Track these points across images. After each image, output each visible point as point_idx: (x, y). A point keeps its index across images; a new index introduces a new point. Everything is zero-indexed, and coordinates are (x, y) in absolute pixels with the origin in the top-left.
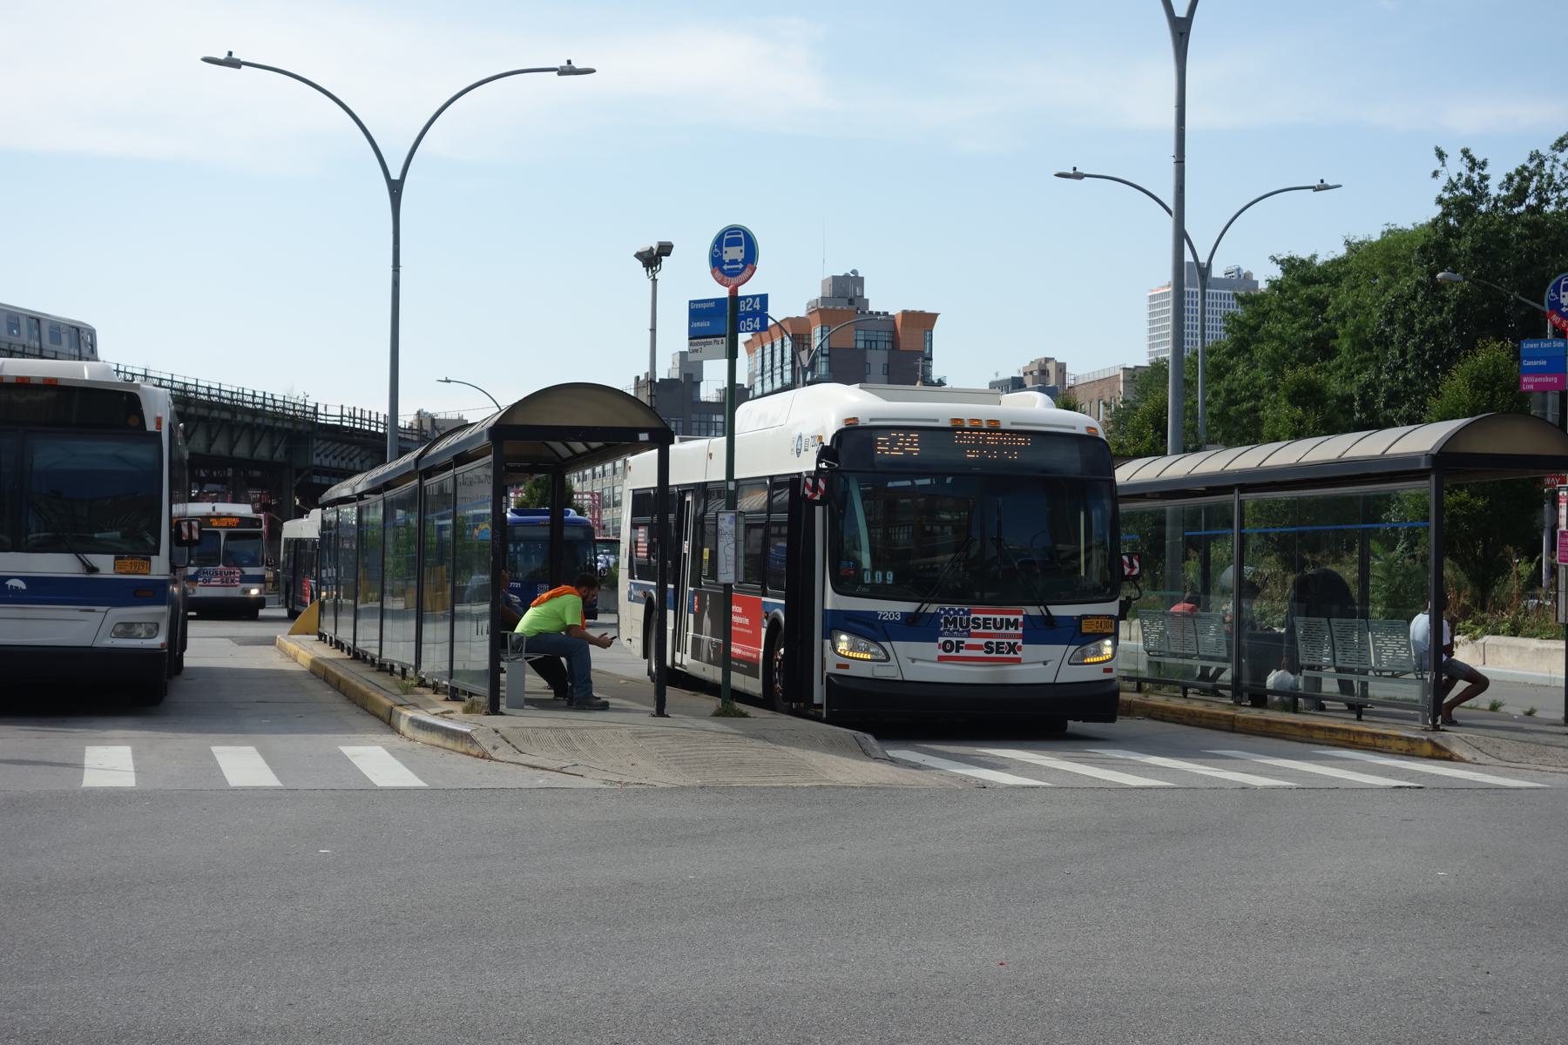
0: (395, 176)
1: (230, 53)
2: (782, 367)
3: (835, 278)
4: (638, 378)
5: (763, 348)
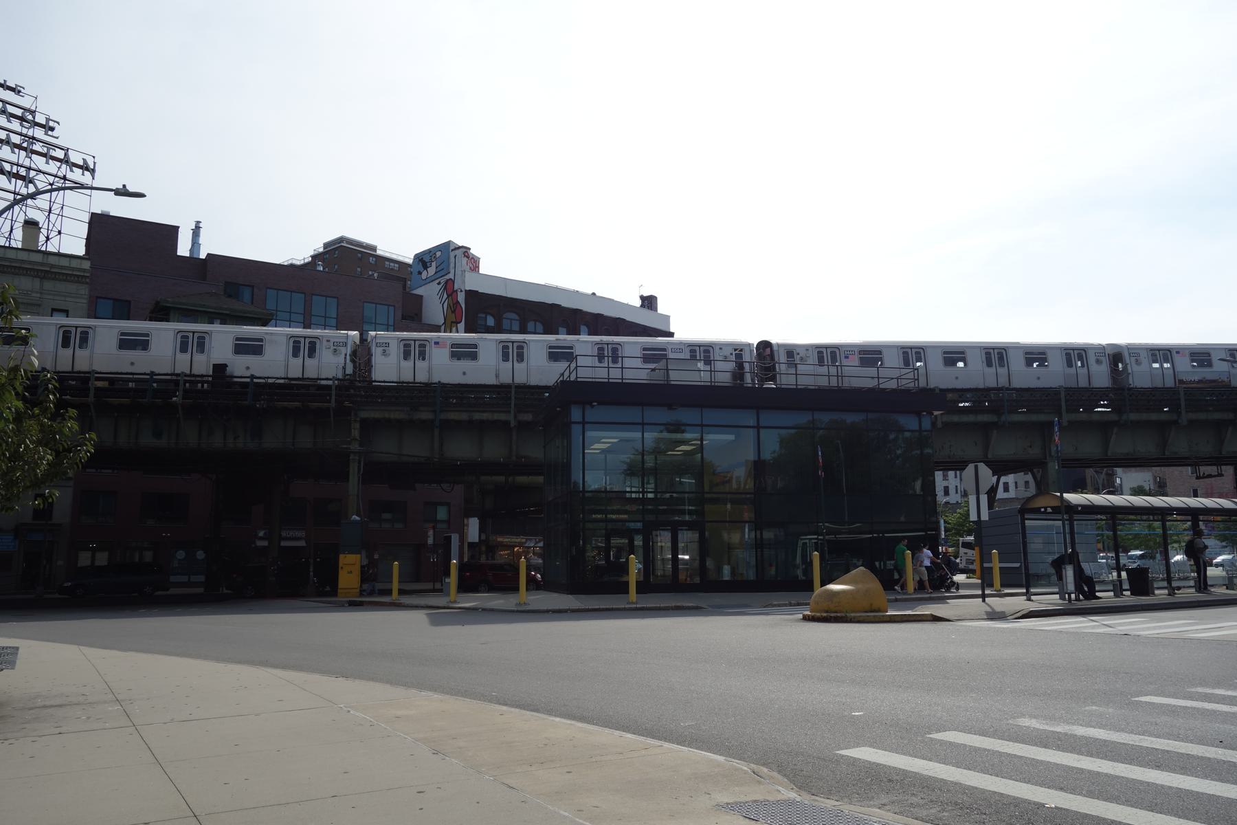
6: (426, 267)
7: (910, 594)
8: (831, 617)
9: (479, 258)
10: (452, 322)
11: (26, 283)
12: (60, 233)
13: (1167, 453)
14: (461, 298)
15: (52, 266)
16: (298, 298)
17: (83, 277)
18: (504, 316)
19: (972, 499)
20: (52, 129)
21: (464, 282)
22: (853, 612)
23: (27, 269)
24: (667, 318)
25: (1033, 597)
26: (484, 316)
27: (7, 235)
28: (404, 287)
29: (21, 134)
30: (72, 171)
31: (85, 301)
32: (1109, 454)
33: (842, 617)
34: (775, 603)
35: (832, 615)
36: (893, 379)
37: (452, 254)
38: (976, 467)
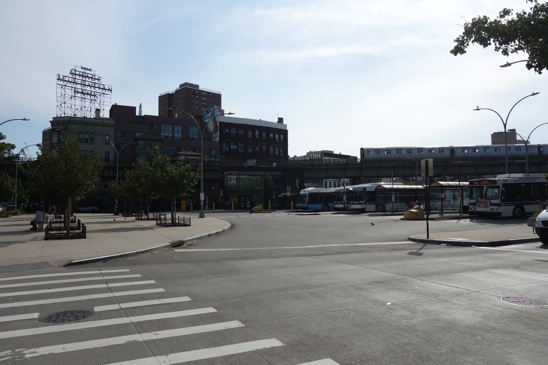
6: (208, 113)
9: (224, 110)
10: (216, 131)
11: (98, 128)
12: (104, 110)
14: (218, 124)
15: (105, 123)
16: (170, 127)
17: (113, 125)
18: (231, 129)
20: (100, 80)
21: (219, 119)
22: (395, 221)
23: (99, 124)
24: (286, 125)
26: (225, 129)
27: (90, 111)
28: (202, 120)
29: (91, 82)
30: (106, 91)
31: (114, 132)
37: (215, 110)
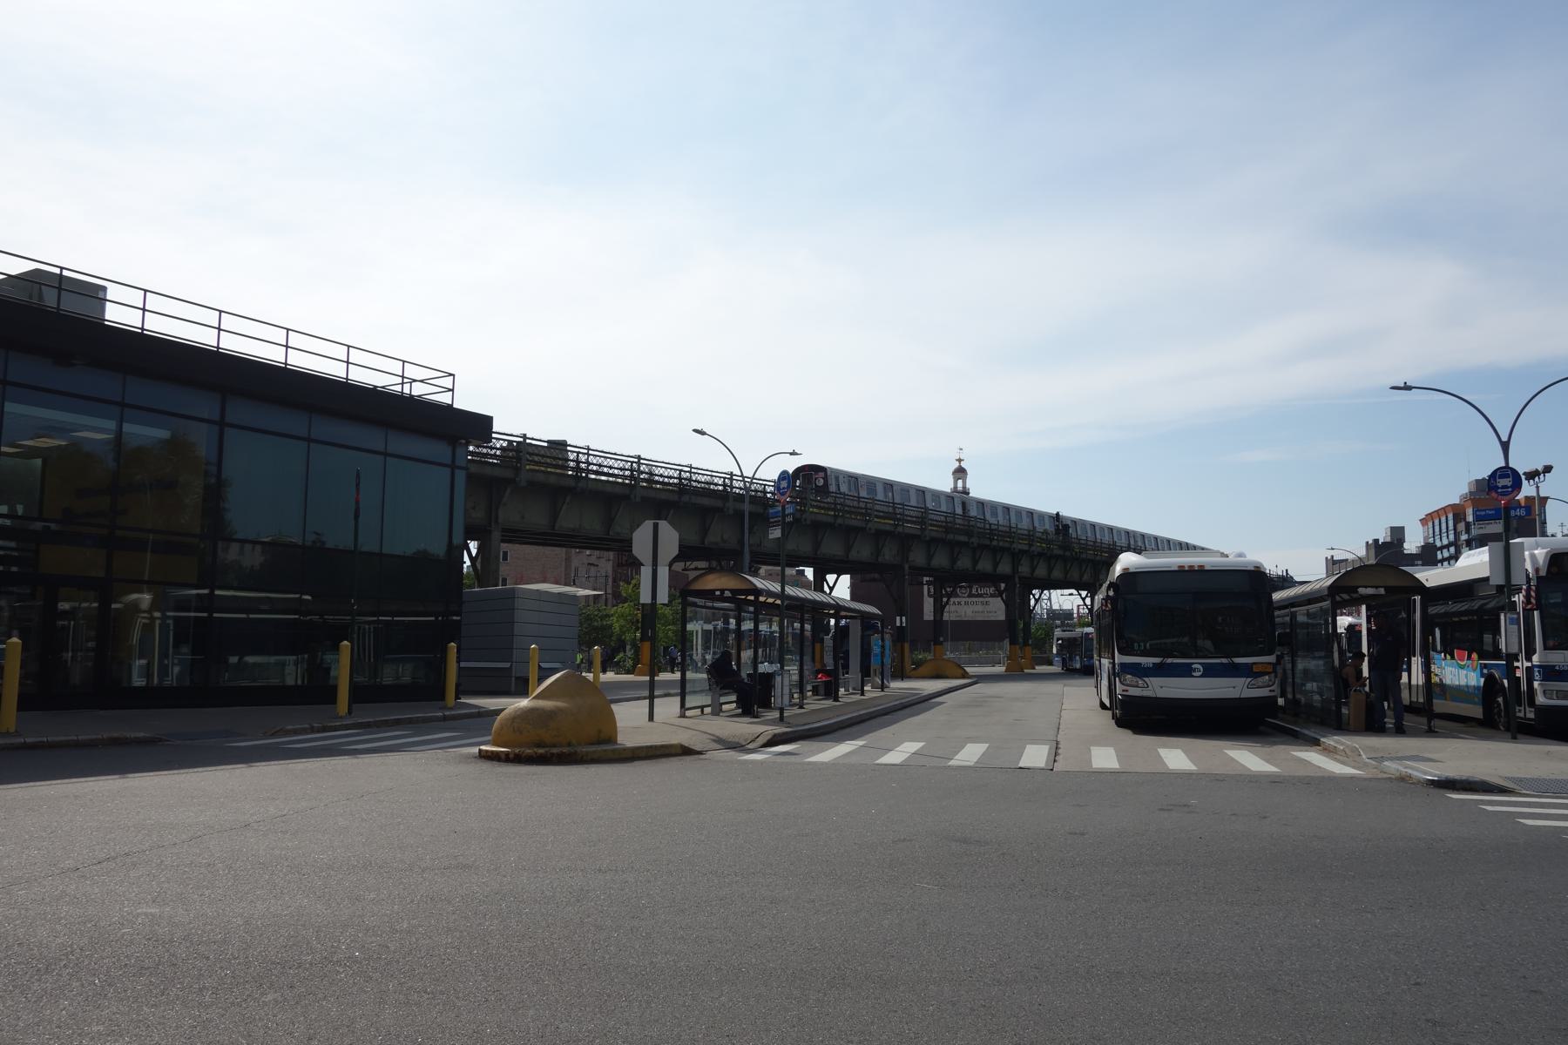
0: (1504, 439)
1: (1405, 383)
2: (1447, 532)
3: (1477, 481)
4: (1367, 543)
5: (1433, 523)
7: (451, 709)
8: (553, 754)
13: (611, 533)
19: (646, 572)
25: (688, 713)
32: (556, 528)
33: (570, 755)
34: (290, 727)
35: (555, 751)
36: (422, 381)
38: (656, 527)
